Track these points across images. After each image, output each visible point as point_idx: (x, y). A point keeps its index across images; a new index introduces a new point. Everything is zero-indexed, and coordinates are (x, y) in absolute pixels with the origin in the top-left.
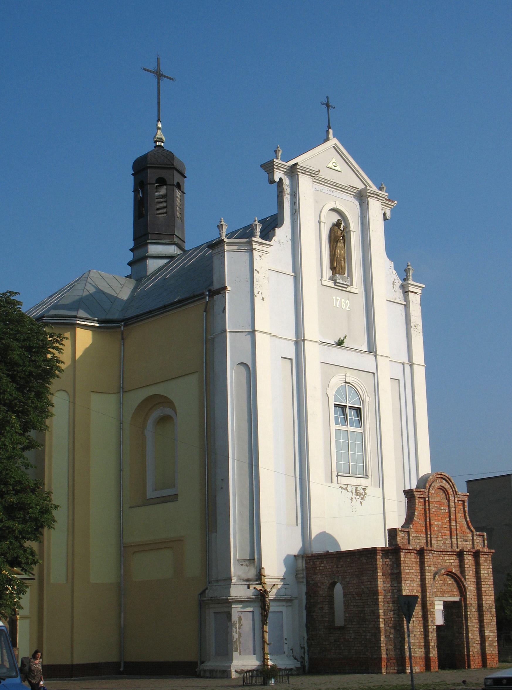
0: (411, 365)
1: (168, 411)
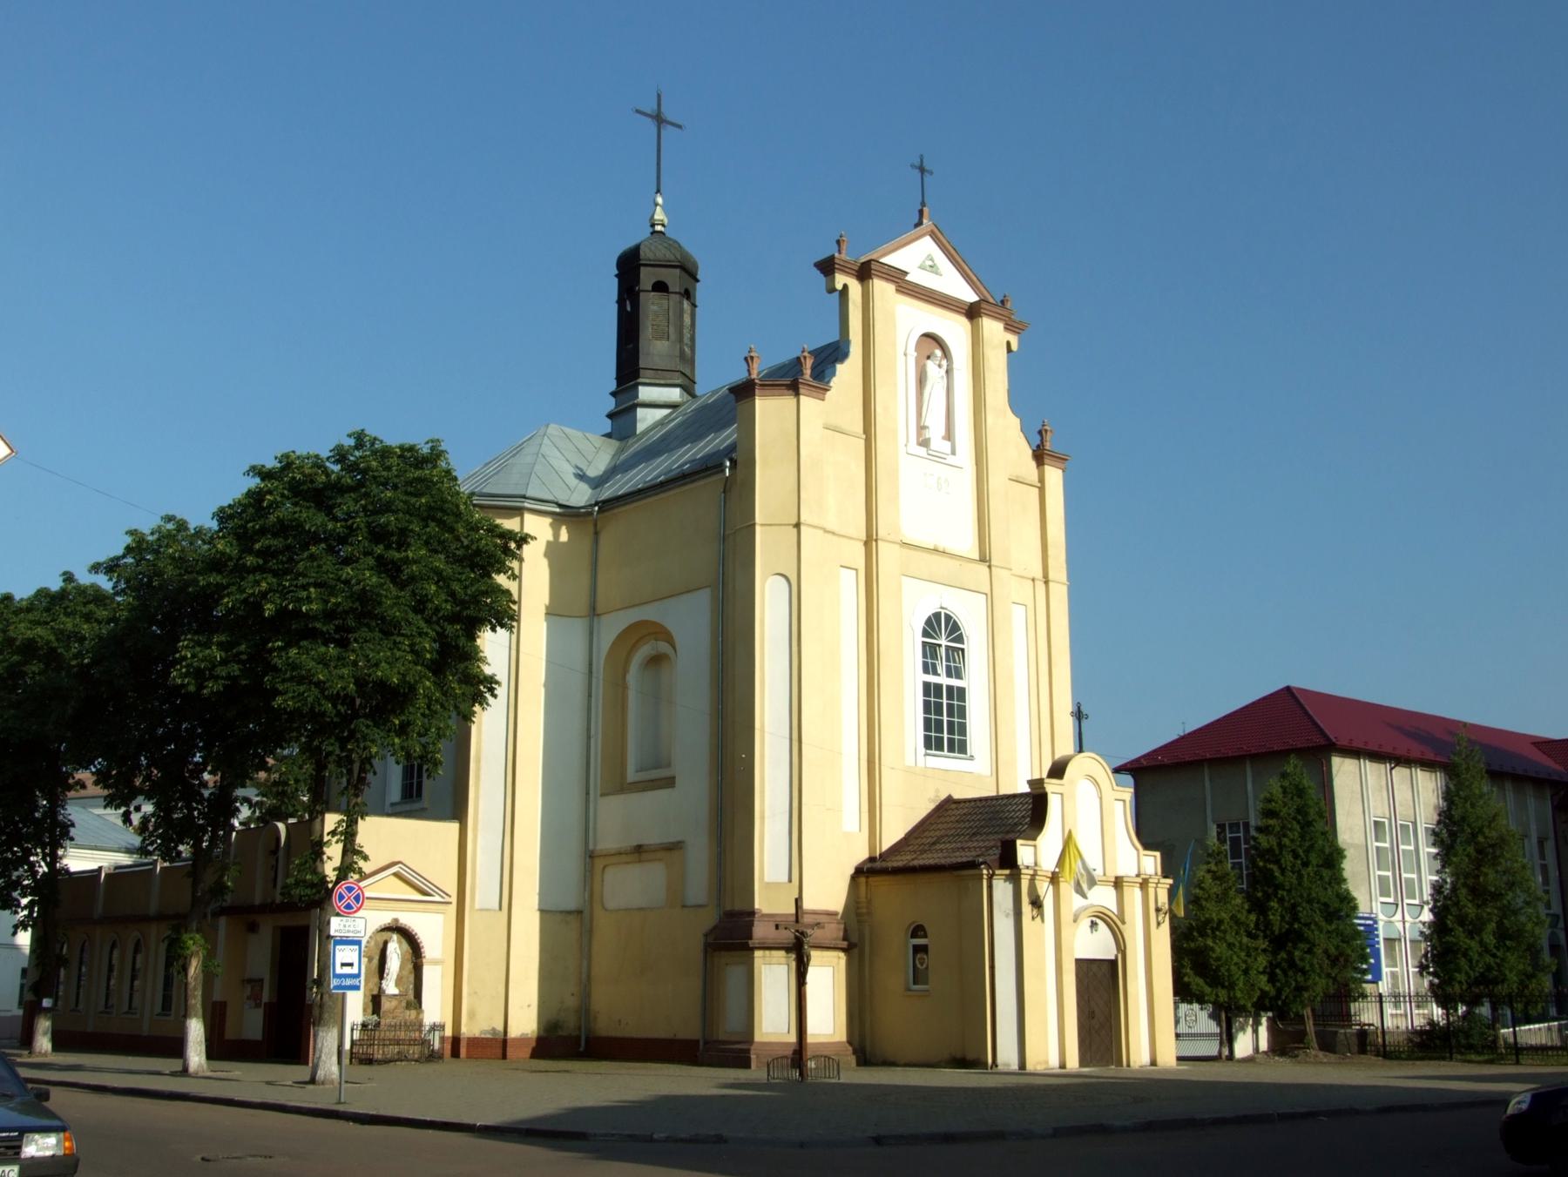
0: (1046, 583)
1: (663, 647)
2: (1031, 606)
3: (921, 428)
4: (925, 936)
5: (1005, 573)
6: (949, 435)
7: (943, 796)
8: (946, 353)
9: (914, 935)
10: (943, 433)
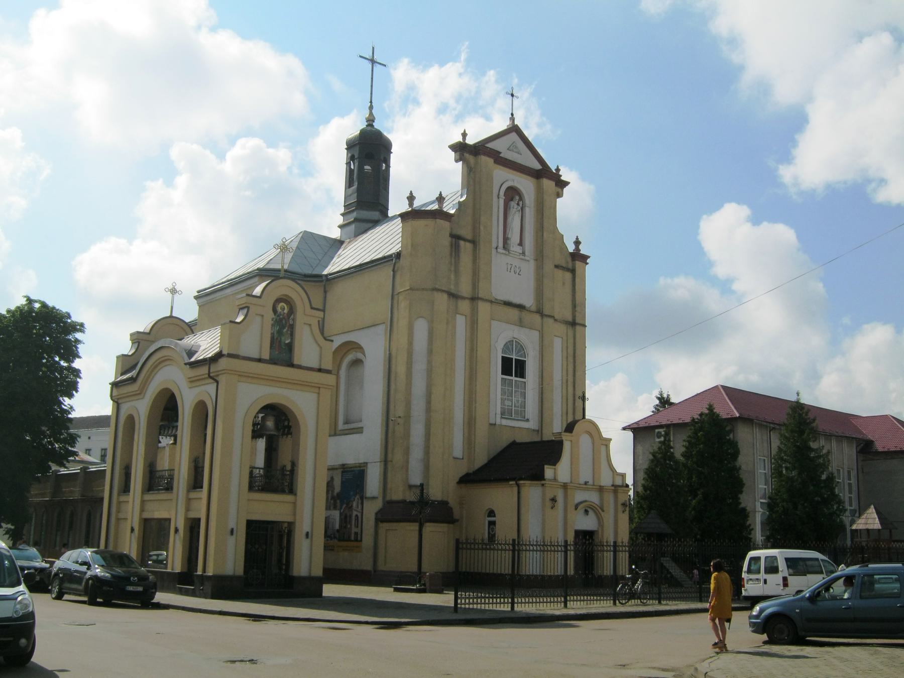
1: (360, 356)
2: (565, 338)
3: (506, 240)
4: (494, 516)
5: (551, 321)
7: (511, 440)
8: (521, 198)
9: (489, 516)
10: (518, 241)
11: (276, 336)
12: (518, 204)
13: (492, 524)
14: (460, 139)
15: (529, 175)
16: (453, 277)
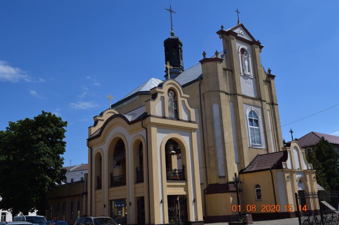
5: (265, 103)
6: (249, 71)
9: (256, 187)
11: (170, 106)
12: (246, 55)
13: (258, 191)
14: (221, 29)
15: (248, 43)
16: (226, 86)
